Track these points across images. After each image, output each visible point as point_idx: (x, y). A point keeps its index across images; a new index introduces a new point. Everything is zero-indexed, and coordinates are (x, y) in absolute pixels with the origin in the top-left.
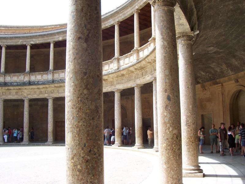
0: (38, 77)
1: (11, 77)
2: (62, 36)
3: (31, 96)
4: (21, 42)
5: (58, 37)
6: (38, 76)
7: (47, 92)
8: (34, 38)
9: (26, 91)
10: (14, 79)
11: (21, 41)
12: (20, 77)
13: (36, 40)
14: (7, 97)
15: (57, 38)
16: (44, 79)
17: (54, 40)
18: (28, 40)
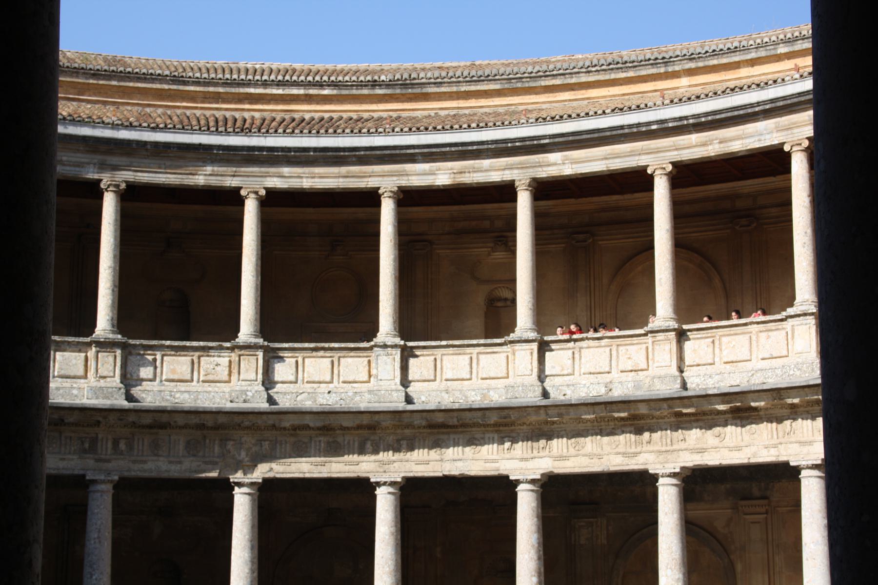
10: (173, 371)
14: (137, 467)
16: (351, 379)
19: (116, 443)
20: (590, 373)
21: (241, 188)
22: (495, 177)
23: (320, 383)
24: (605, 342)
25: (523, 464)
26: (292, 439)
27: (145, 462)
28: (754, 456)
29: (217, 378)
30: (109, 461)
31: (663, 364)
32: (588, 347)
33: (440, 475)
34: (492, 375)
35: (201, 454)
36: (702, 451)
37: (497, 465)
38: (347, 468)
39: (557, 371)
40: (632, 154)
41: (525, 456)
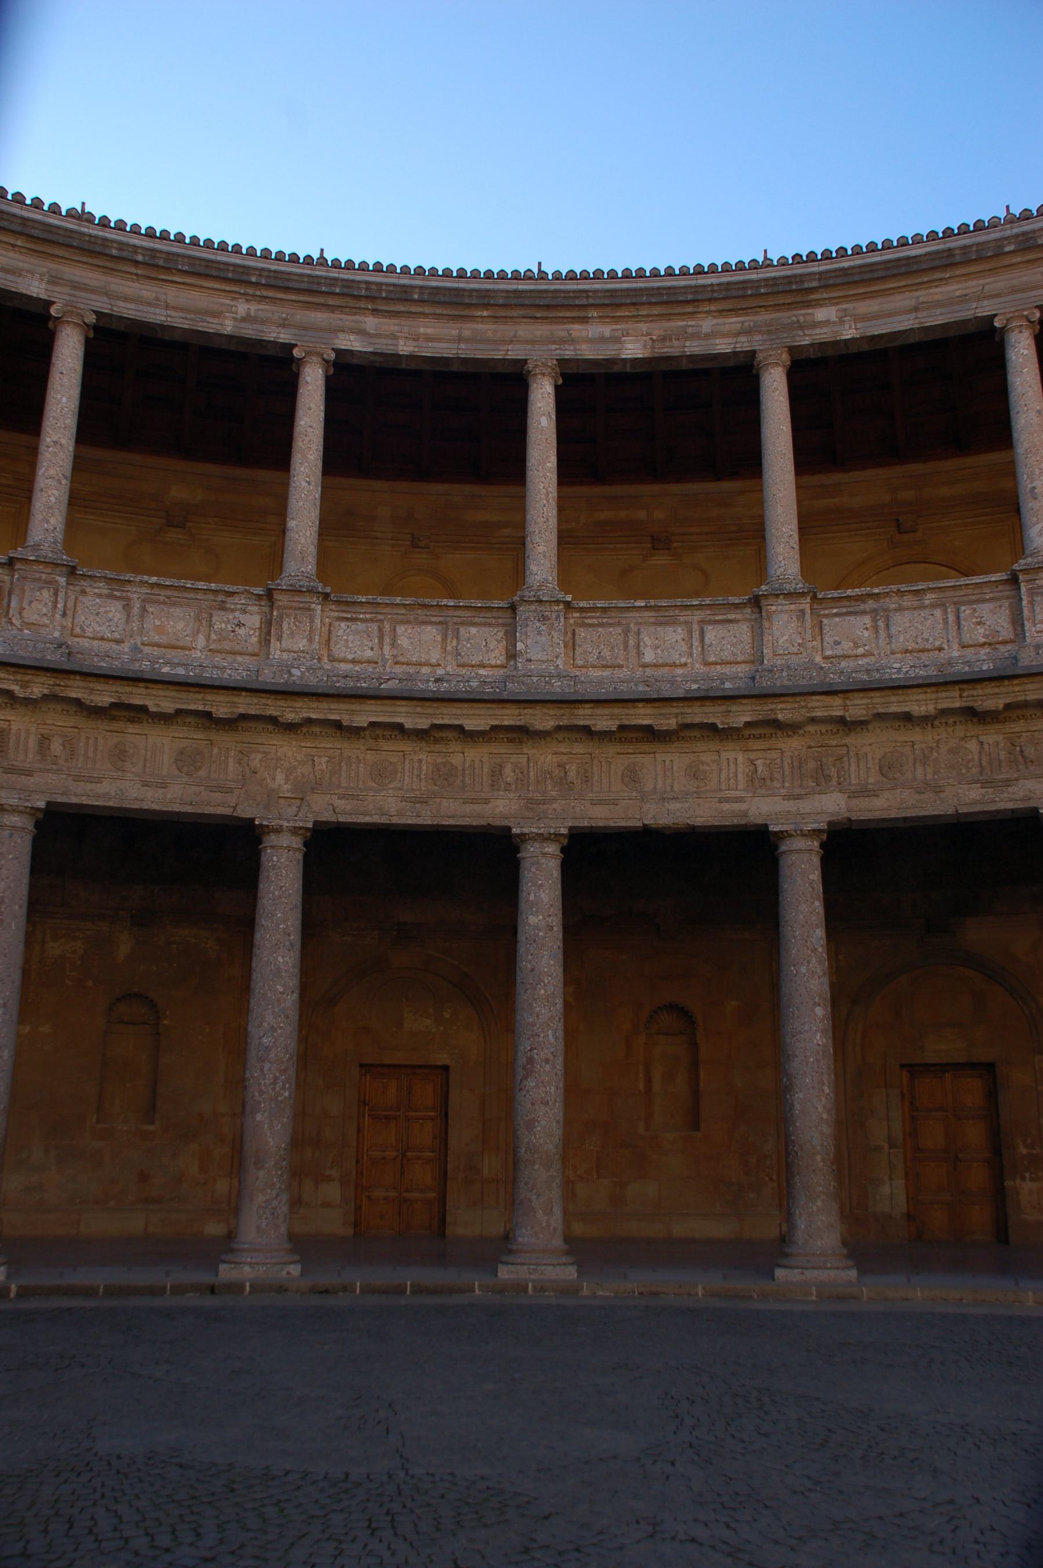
0: (403, 642)
1: (127, 608)
2: (644, 327)
3: (340, 804)
4: (247, 319)
5: (606, 330)
6: (400, 629)
8: (375, 312)
9: (288, 749)
10: (160, 630)
11: (242, 308)
12: (221, 622)
13: (389, 325)
14: (82, 787)
15: (602, 339)
17: (568, 353)
18: (319, 317)
19: (44, 740)
20: (907, 651)
21: (296, 345)
22: (723, 346)
23: (420, 664)
24: (929, 598)
25: (790, 806)
26: (371, 756)
27: (99, 780)
29: (238, 648)
30: (29, 773)
32: (900, 609)
33: (639, 824)
34: (726, 655)
35: (202, 773)
37: (743, 806)
38: (468, 808)
39: (846, 646)
40: (964, 299)
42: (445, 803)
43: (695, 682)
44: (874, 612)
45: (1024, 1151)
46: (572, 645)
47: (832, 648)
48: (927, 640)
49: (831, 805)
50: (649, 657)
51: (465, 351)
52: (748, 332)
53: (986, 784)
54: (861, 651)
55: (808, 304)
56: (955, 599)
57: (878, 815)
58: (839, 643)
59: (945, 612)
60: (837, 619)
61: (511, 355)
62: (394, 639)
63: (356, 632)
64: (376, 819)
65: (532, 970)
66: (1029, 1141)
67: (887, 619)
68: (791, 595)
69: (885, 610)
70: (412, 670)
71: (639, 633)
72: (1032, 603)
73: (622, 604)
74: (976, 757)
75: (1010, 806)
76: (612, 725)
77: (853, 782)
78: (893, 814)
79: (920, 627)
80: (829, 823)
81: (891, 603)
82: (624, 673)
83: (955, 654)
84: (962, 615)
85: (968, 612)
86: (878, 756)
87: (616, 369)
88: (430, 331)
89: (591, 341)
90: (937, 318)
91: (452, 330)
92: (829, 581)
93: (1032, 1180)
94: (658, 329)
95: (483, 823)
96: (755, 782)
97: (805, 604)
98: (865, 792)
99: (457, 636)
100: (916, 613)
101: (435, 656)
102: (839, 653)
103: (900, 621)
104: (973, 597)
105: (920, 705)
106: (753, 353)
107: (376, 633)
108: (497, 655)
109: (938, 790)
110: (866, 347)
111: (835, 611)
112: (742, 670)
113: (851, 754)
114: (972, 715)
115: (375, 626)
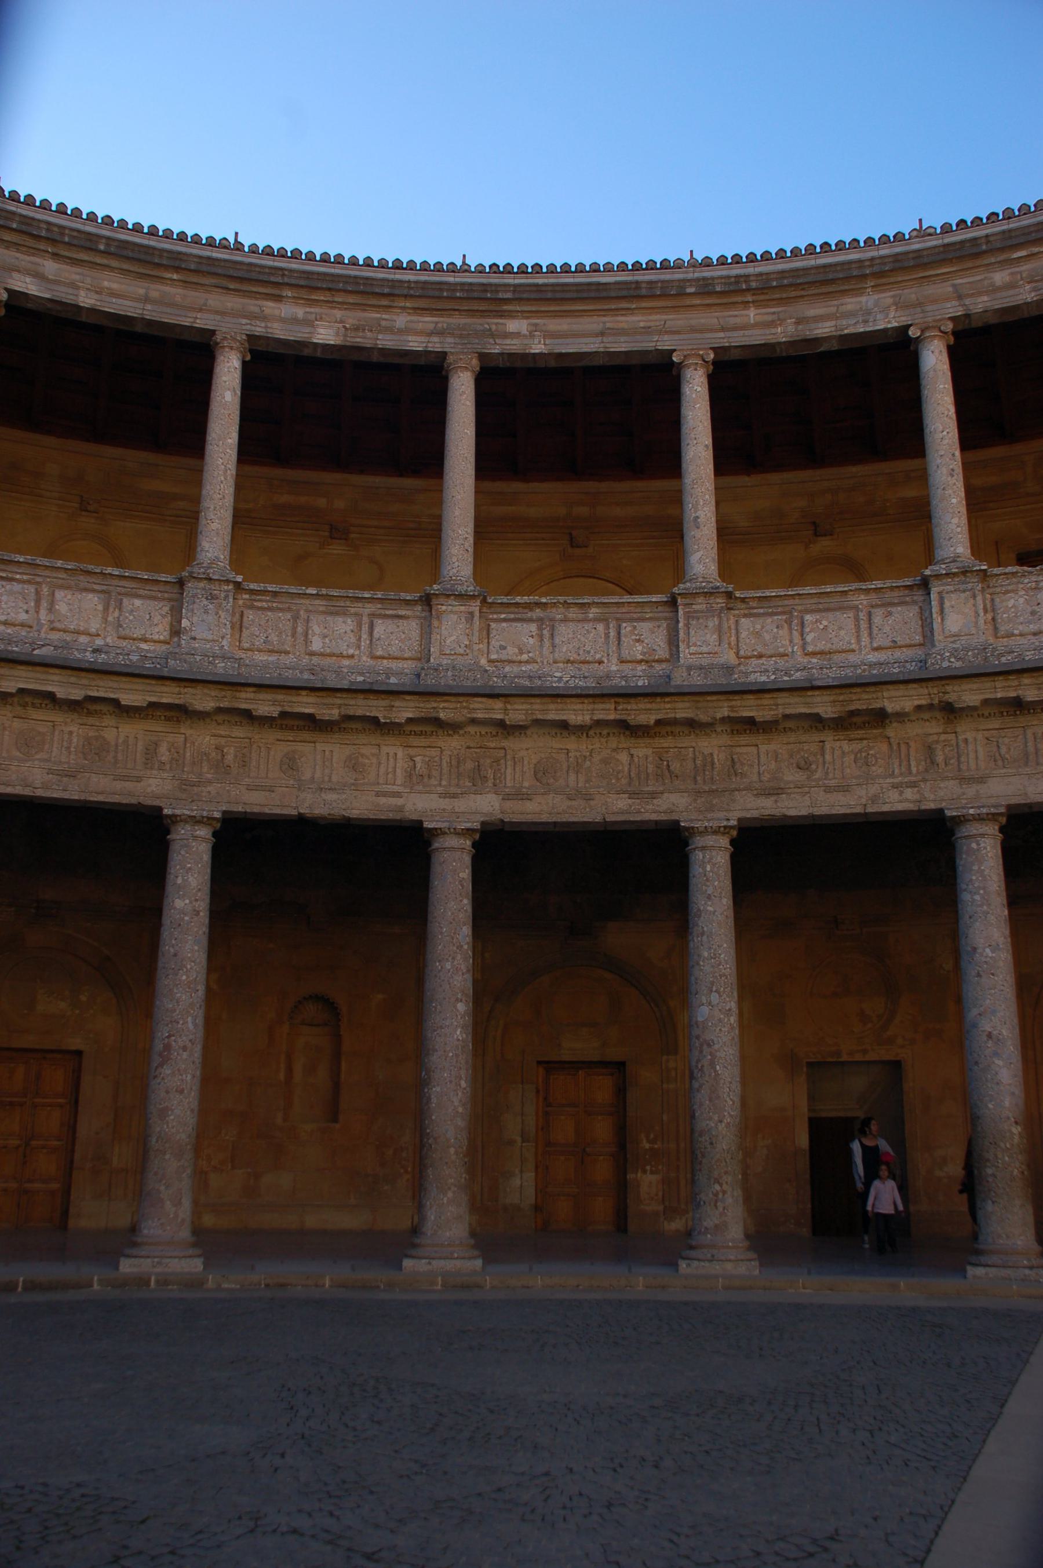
0: (62, 607)
2: (338, 314)
5: (300, 312)
6: (59, 594)
7: (164, 753)
13: (71, 273)
15: (295, 321)
17: (259, 329)
20: (568, 661)
22: (415, 343)
23: (78, 633)
25: (446, 804)
26: (17, 724)
28: (874, 799)
31: (705, 649)
32: (565, 620)
33: (294, 812)
34: (394, 650)
36: (775, 792)
37: (400, 802)
38: (119, 785)
39: (511, 652)
40: (647, 331)
41: (453, 790)
42: (94, 778)
43: (362, 674)
44: (540, 620)
45: (647, 1146)
46: (239, 626)
47: (497, 652)
48: (589, 652)
49: (486, 806)
50: (316, 645)
51: (151, 312)
52: (441, 333)
53: (632, 795)
54: (525, 657)
55: (501, 314)
56: (618, 616)
57: (530, 818)
58: (505, 648)
59: (607, 627)
60: (504, 624)
61: (199, 324)
62: (52, 603)
63: (11, 593)
64: (18, 790)
65: (175, 955)
66: (652, 1136)
67: (553, 628)
68: (462, 597)
69: (551, 620)
70: (68, 638)
71: (308, 621)
72: (687, 626)
73: (293, 590)
74: (626, 769)
75: (654, 817)
76: (274, 711)
77: (509, 784)
78: (544, 818)
79: (583, 639)
80: (483, 823)
81: (558, 614)
82: (288, 660)
83: (614, 668)
84: (623, 631)
85: (629, 629)
86: (534, 761)
87: (307, 352)
88: (115, 286)
89: (283, 320)
90: (621, 345)
91: (139, 288)
92: (500, 587)
93: (652, 1172)
94: (353, 317)
95: (134, 801)
96: (414, 779)
97: (475, 607)
98: (520, 795)
99: (120, 606)
100: (580, 625)
101: (94, 626)
102: (504, 657)
103: (564, 631)
104: (635, 616)
105: (577, 714)
106: (444, 355)
107: (33, 596)
108: (160, 630)
109: (588, 798)
110: (553, 364)
111: (503, 616)
112: (408, 666)
113: (508, 757)
114: (624, 726)
115: (32, 589)
